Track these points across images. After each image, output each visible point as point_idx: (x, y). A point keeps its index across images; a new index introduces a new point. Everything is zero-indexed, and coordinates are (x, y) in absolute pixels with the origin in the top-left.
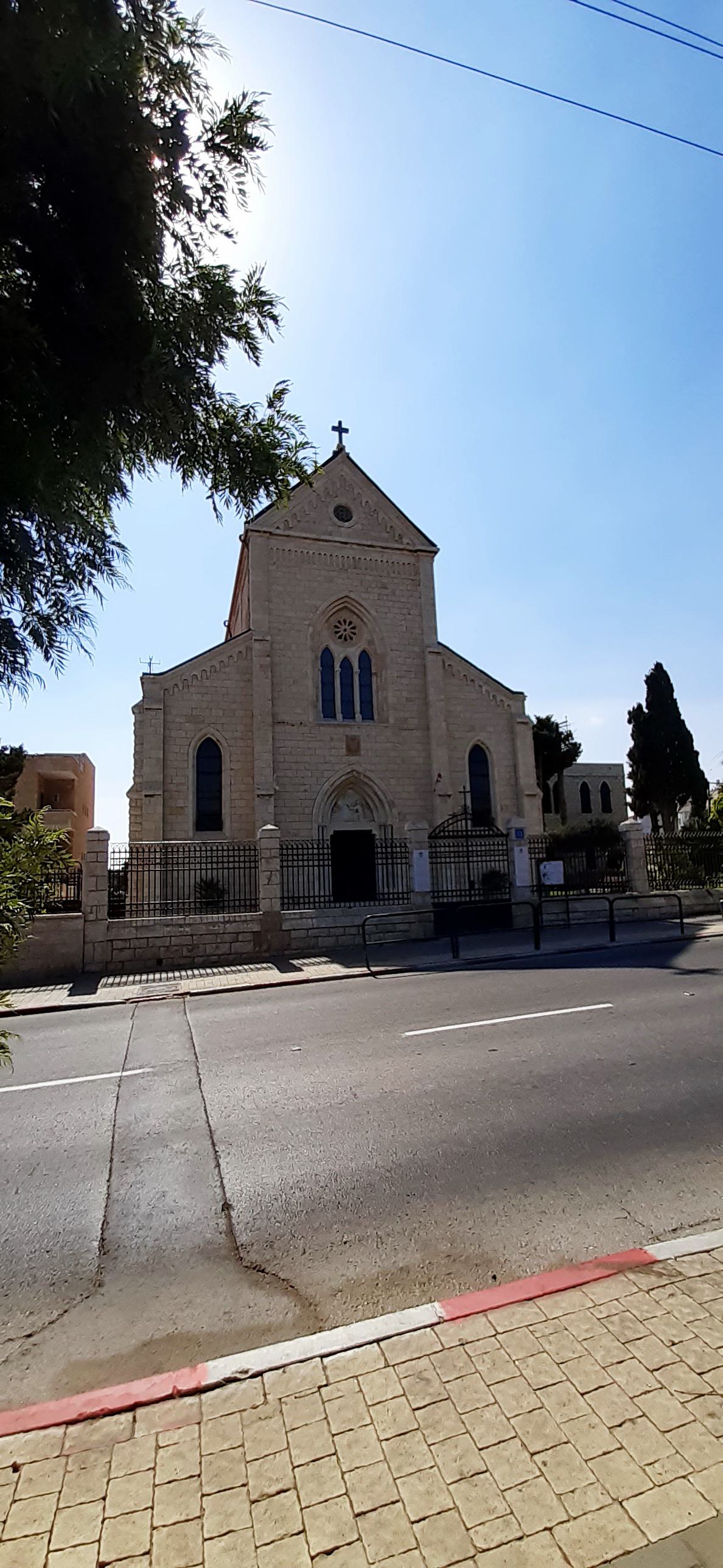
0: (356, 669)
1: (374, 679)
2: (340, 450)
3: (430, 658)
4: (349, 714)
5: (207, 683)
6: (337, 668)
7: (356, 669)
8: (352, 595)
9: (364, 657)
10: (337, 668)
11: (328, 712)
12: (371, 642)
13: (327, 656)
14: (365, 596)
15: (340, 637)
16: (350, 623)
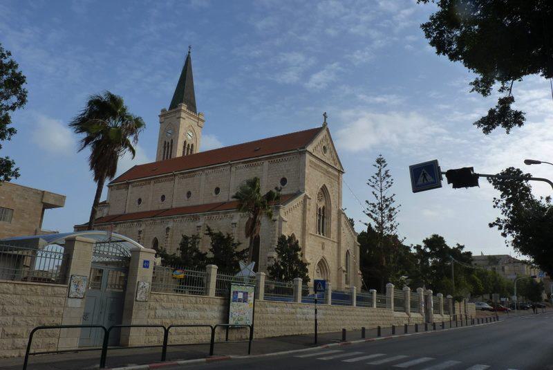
2: (325, 124)
3: (342, 215)
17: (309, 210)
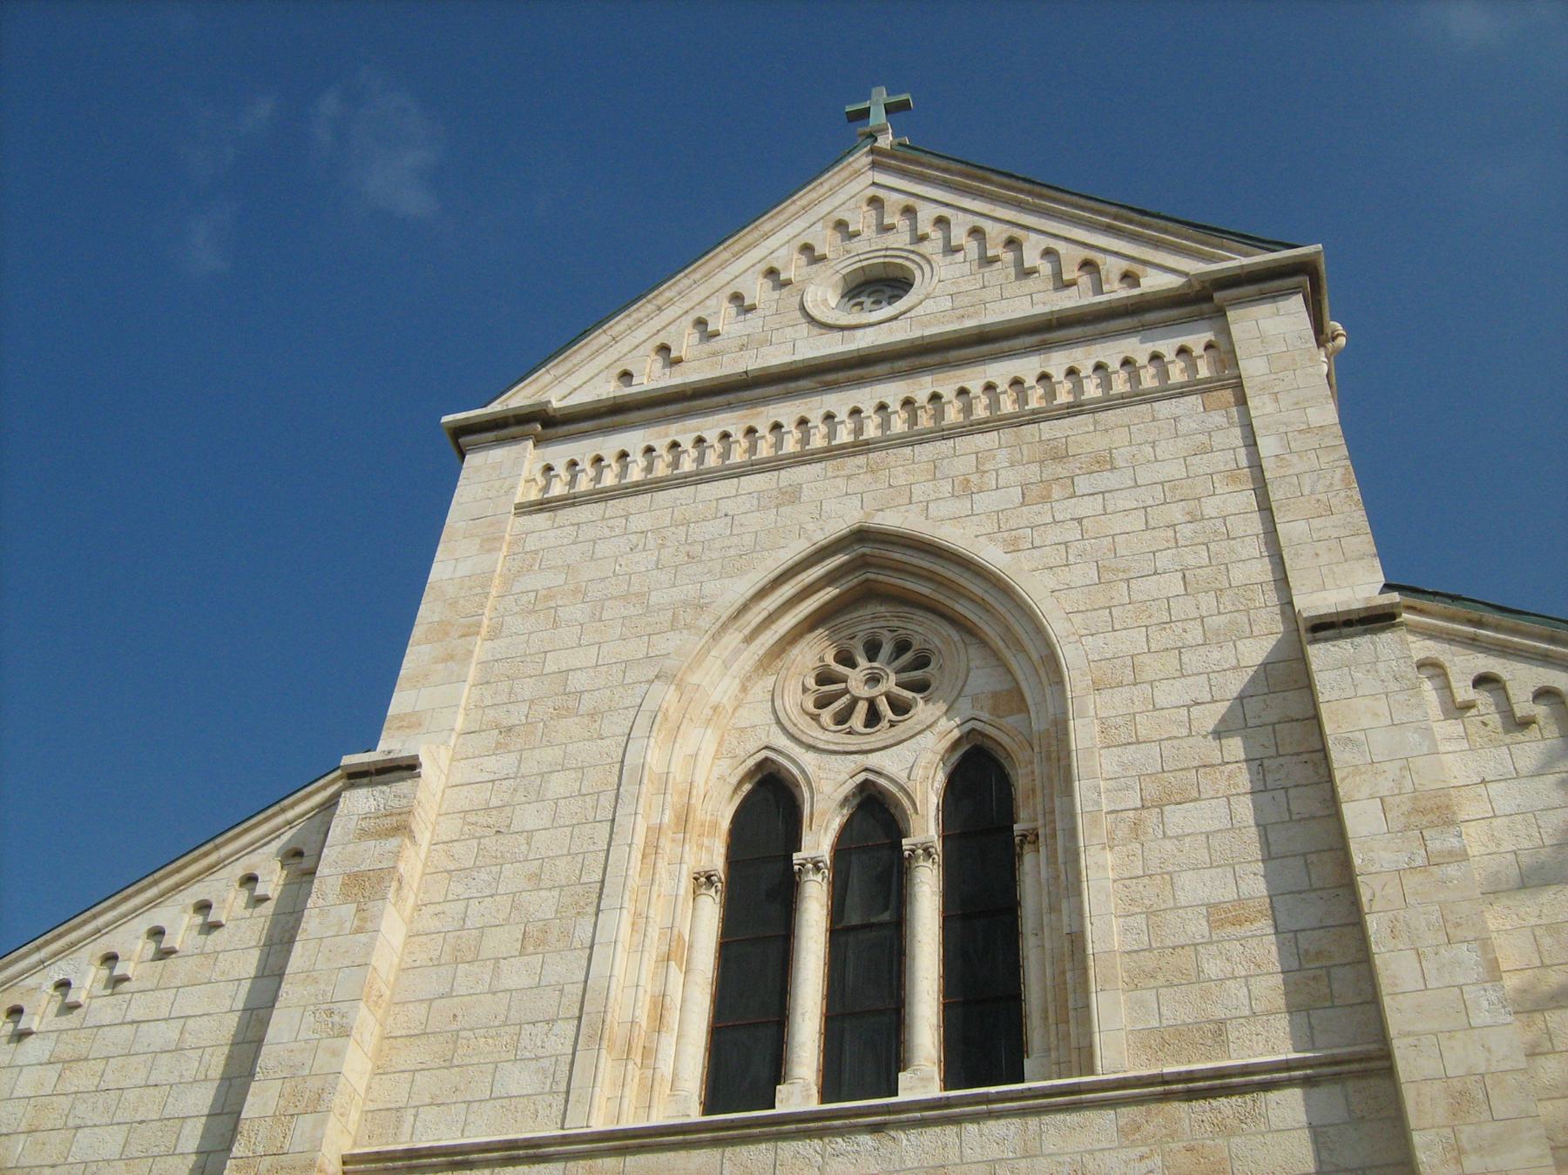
5: (104, 1009)
8: (891, 520)
12: (1013, 699)
14: (963, 506)
16: (902, 647)
17: (367, 886)
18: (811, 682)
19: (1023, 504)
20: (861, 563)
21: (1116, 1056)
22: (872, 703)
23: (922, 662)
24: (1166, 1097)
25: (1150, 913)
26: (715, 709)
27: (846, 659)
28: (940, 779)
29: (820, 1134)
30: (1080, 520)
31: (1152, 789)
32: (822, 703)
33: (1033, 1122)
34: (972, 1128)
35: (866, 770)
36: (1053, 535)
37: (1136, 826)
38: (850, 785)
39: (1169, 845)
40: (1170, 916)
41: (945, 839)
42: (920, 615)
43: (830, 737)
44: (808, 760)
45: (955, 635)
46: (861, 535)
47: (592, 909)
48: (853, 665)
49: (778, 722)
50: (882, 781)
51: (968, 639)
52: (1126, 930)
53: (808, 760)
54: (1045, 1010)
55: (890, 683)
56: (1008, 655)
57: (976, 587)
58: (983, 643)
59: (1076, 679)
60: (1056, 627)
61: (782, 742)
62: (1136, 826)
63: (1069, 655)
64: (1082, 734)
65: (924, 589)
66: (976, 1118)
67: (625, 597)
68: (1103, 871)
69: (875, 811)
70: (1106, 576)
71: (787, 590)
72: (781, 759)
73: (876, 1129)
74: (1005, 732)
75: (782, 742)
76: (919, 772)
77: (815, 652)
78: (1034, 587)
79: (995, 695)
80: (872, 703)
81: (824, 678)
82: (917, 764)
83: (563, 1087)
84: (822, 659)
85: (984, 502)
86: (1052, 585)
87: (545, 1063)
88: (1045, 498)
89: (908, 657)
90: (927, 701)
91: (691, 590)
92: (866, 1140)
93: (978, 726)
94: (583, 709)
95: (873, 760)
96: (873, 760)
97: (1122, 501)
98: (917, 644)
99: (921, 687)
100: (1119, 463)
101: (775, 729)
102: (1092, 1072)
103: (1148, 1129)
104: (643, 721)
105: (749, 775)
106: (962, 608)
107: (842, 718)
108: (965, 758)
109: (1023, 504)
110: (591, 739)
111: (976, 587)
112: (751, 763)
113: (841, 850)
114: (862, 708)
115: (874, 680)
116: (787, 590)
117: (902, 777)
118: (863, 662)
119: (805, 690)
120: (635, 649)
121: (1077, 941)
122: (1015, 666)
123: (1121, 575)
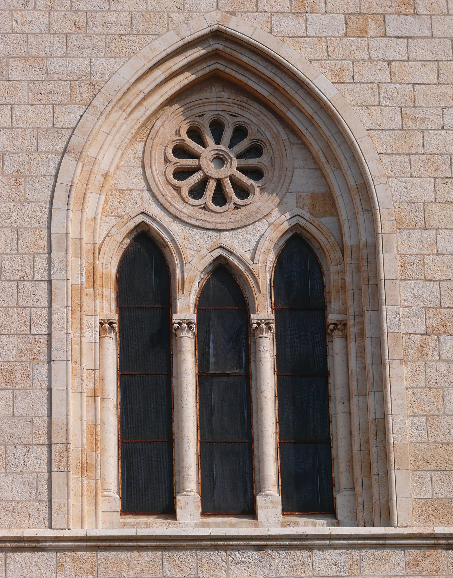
0: (263, 310)
1: (336, 345)
4: (231, 490)
6: (185, 308)
7: (263, 310)
8: (243, 27)
9: (299, 258)
10: (185, 308)
11: (147, 484)
12: (325, 202)
13: (145, 263)
15: (197, 191)
16: (240, 132)
18: (170, 152)
19: (346, 35)
20: (214, 55)
21: (407, 520)
22: (219, 182)
23: (255, 150)
24: (434, 546)
25: (429, 416)
26: (106, 176)
27: (195, 134)
28: (272, 258)
29: (225, 548)
30: (389, 62)
31: (434, 321)
32: (182, 174)
33: (356, 553)
34: (319, 554)
35: (221, 247)
36: (368, 73)
37: (422, 347)
38: (209, 259)
39: (442, 366)
40: (441, 420)
41: (277, 311)
42: (256, 108)
43: (189, 209)
44: (176, 228)
45: (283, 134)
46: (217, 34)
47: (44, 357)
48: (204, 144)
49: (150, 189)
50: (232, 259)
51: (293, 139)
52: (414, 426)
53: (176, 228)
54: (351, 461)
55: (232, 168)
56: (328, 169)
57: (308, 107)
58: (305, 145)
59: (386, 221)
60: (373, 167)
61: (155, 210)
62: (422, 347)
63: (383, 194)
64: (389, 267)
65: (263, 90)
66: (321, 548)
67: (26, 58)
68: (400, 377)
69: (224, 276)
70: (409, 124)
71: (159, 75)
72: (154, 225)
73: (259, 548)
74: (321, 231)
75: (155, 210)
76: (259, 257)
77: (172, 126)
78: (355, 123)
79: (313, 196)
80: (219, 182)
81: (180, 151)
82: (254, 239)
83: (45, 497)
84: (178, 133)
85: (319, 25)
86: (368, 123)
87: (30, 477)
88: (363, 33)
89: (244, 144)
90: (263, 189)
91: (82, 64)
92: (253, 554)
93: (302, 222)
94: (7, 171)
95: (226, 239)
96: (226, 239)
97: (422, 50)
98: (252, 130)
99: (256, 174)
100: (421, 9)
101: (147, 195)
102: (389, 523)
103: (424, 565)
104: (60, 194)
105: (128, 236)
106: (292, 116)
107: (182, 174)
108: (289, 241)
109: (346, 35)
110: (18, 201)
111: (308, 107)
112: (132, 225)
113: (201, 307)
114: (212, 185)
115: (220, 160)
116: (159, 75)
117: (247, 257)
118: (210, 140)
119: (167, 161)
120: (41, 116)
121: (381, 426)
122: (332, 178)
123: (419, 126)
